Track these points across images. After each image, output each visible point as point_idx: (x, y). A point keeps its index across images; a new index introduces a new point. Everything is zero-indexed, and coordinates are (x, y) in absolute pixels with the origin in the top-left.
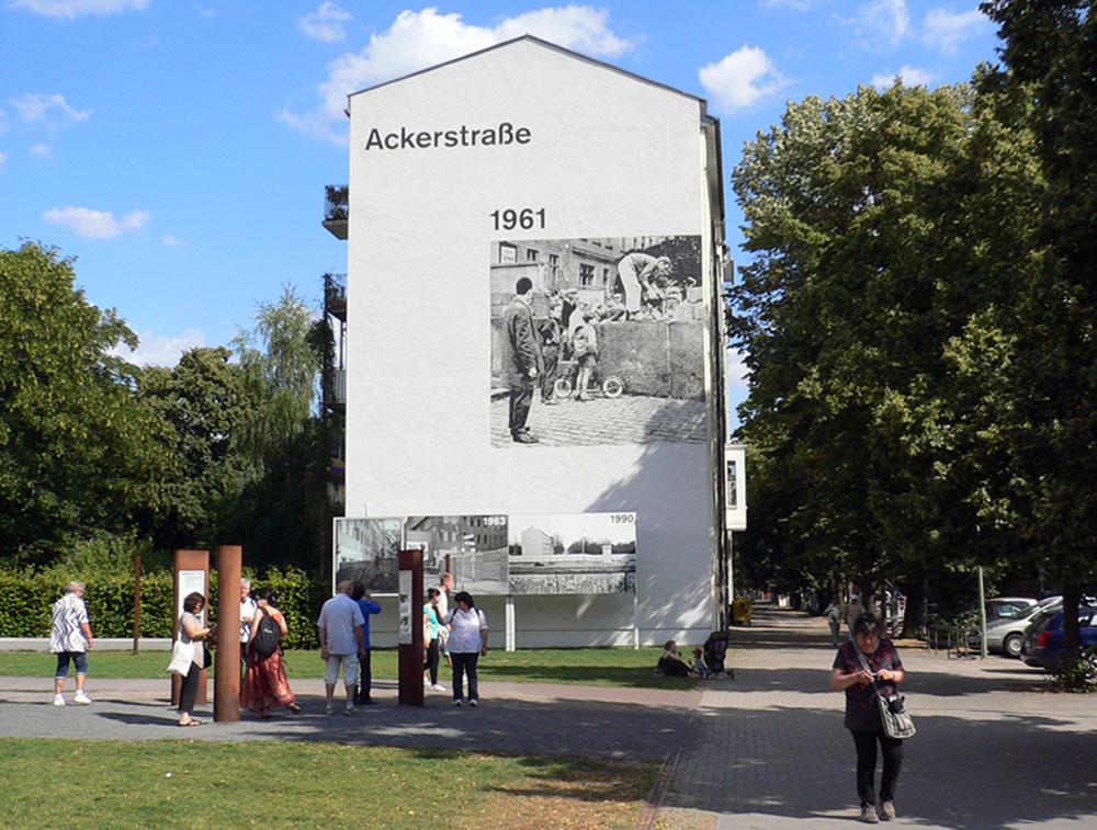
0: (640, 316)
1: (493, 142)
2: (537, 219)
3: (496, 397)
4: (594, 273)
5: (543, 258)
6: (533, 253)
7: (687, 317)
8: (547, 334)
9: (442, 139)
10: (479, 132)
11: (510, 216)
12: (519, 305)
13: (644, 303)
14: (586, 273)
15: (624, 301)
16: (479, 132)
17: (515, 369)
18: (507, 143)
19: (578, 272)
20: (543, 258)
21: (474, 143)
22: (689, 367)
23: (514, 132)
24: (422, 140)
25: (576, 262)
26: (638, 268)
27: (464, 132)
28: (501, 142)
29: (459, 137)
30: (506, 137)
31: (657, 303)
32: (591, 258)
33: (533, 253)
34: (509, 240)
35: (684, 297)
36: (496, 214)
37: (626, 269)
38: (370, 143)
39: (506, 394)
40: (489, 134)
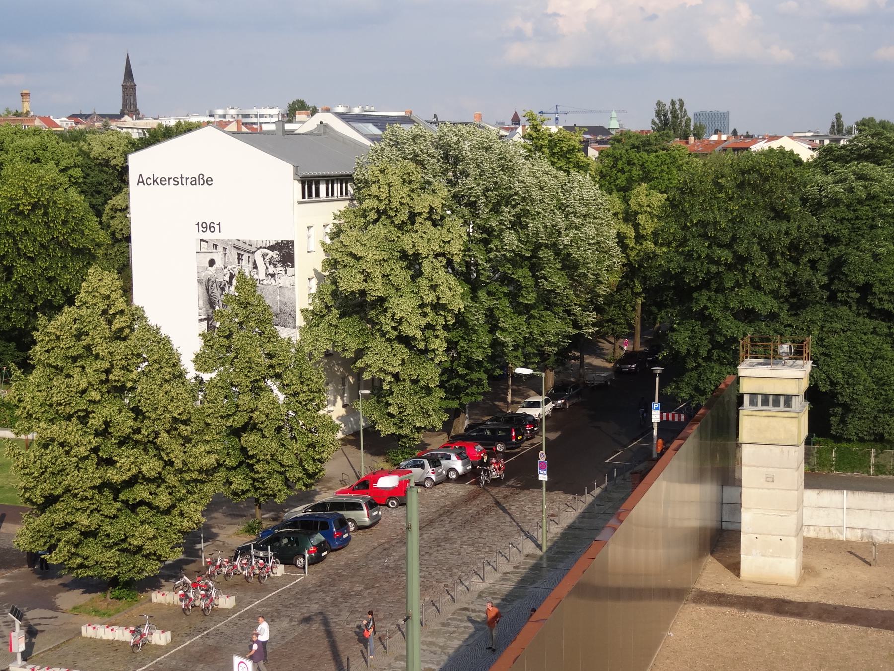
0: (265, 282)
2: (217, 227)
3: (201, 320)
4: (244, 258)
5: (220, 249)
6: (215, 246)
7: (287, 285)
8: (223, 289)
9: (172, 181)
11: (204, 225)
12: (210, 273)
13: (267, 275)
14: (240, 258)
15: (257, 274)
17: (208, 306)
19: (236, 257)
20: (220, 249)
22: (288, 311)
24: (163, 182)
25: (236, 251)
26: (264, 256)
27: (182, 178)
29: (179, 180)
30: (201, 182)
31: (273, 276)
32: (242, 250)
33: (215, 246)
34: (204, 238)
35: (285, 271)
36: (198, 224)
37: (258, 256)
38: (139, 182)
39: (205, 319)
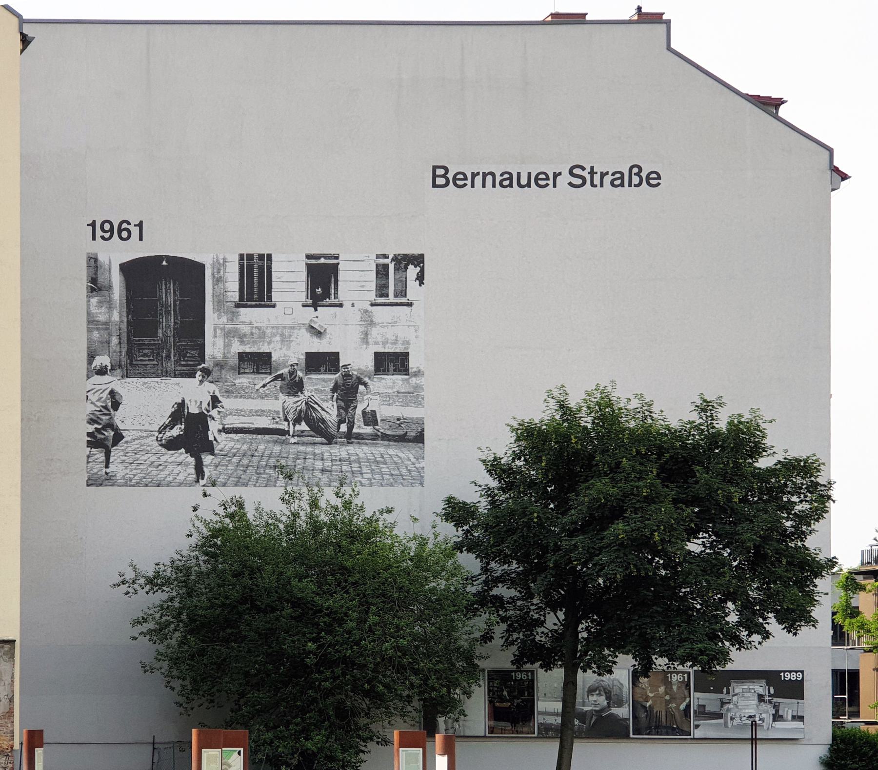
1: (622, 185)
10: (607, 173)
16: (607, 173)
18: (635, 186)
21: (602, 186)
23: (644, 175)
27: (592, 173)
28: (630, 185)
30: (636, 180)
40: (618, 175)
